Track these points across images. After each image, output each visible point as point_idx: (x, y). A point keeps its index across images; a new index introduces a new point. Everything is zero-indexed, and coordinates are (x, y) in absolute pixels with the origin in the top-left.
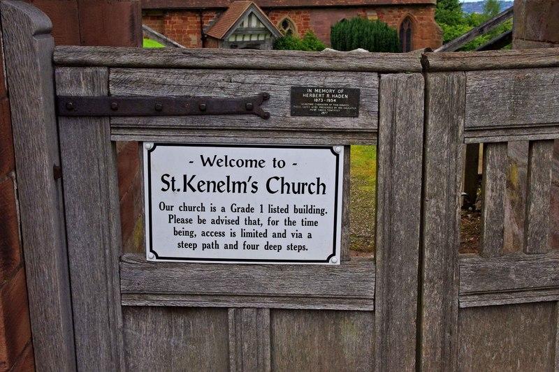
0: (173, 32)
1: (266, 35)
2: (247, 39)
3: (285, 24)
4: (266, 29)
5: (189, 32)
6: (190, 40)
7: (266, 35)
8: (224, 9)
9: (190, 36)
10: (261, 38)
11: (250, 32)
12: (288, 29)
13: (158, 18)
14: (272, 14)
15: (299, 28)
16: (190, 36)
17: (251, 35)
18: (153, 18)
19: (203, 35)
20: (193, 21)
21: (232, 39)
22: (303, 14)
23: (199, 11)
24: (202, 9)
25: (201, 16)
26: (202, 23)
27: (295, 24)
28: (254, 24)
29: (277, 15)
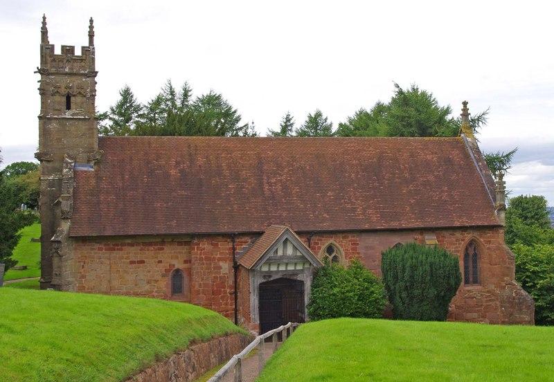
0: (201, 259)
1: (304, 264)
2: (282, 268)
3: (330, 250)
4: (303, 257)
5: (220, 259)
6: (220, 268)
7: (304, 264)
8: (260, 234)
9: (221, 264)
10: (299, 267)
11: (285, 261)
12: (333, 255)
13: (187, 243)
14: (314, 239)
15: (346, 253)
16: (221, 264)
17: (287, 264)
18: (180, 243)
19: (235, 263)
20: (224, 246)
21: (265, 269)
22: (350, 238)
23: (231, 236)
24: (234, 234)
25: (234, 242)
26: (234, 249)
27: (341, 249)
28: (290, 251)
29: (321, 240)
